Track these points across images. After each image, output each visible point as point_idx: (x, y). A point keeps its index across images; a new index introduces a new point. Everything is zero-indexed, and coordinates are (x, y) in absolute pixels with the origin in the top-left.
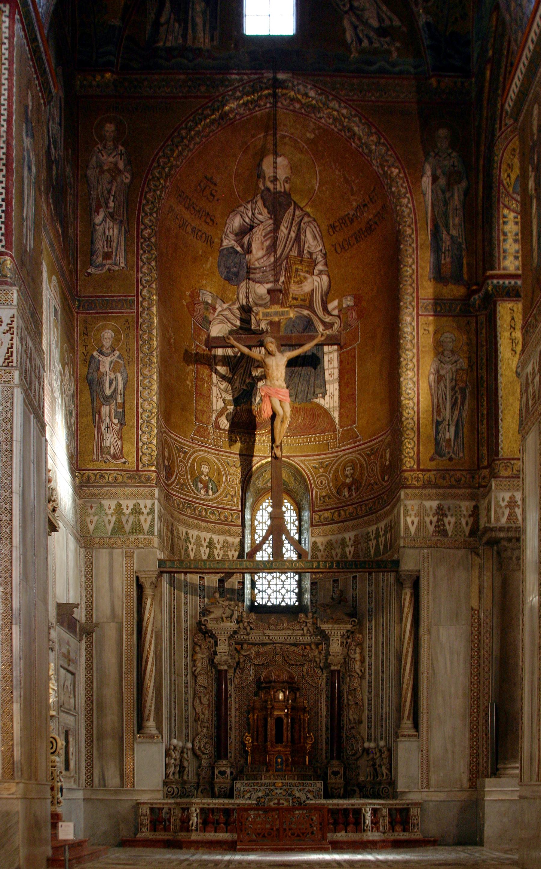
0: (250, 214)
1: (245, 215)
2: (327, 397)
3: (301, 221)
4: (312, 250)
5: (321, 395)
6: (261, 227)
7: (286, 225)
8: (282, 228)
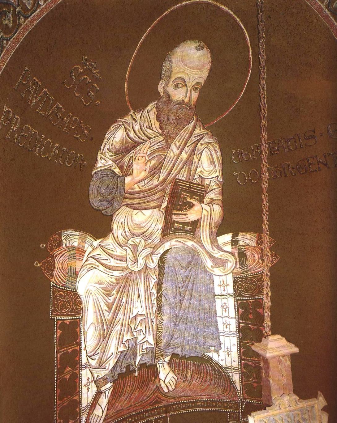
0: (137, 128)
1: (130, 128)
2: (221, 352)
3: (199, 141)
4: (205, 175)
5: (213, 348)
6: (148, 144)
7: (178, 144)
8: (173, 147)
